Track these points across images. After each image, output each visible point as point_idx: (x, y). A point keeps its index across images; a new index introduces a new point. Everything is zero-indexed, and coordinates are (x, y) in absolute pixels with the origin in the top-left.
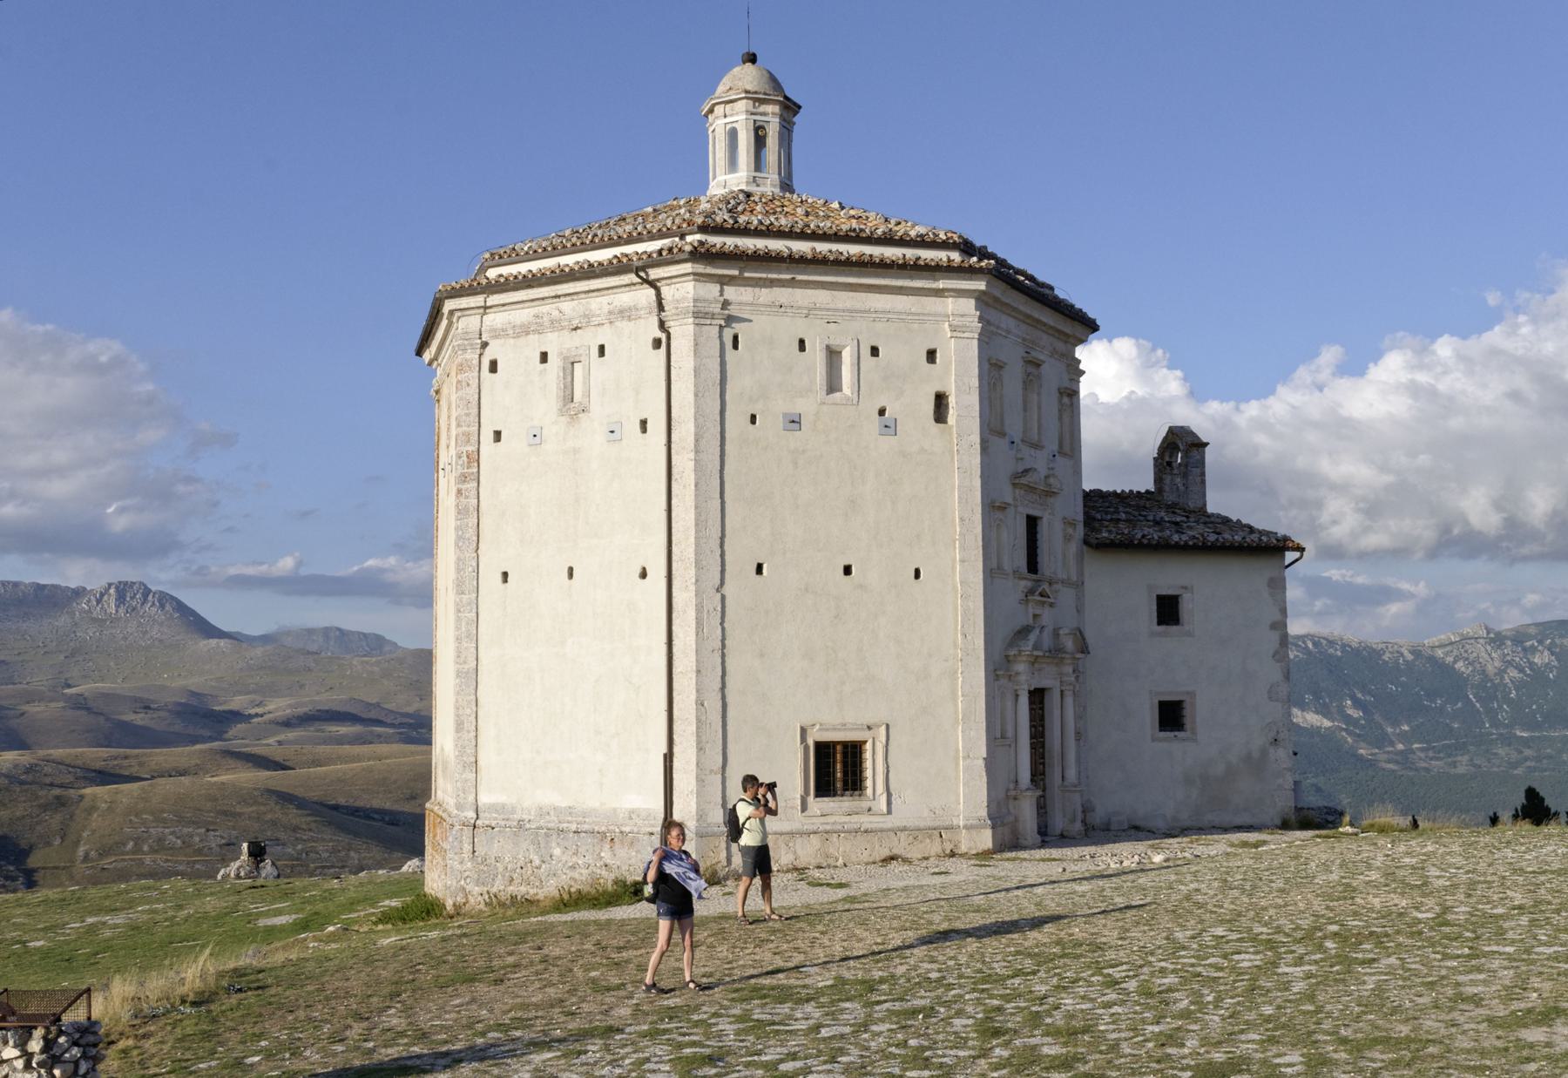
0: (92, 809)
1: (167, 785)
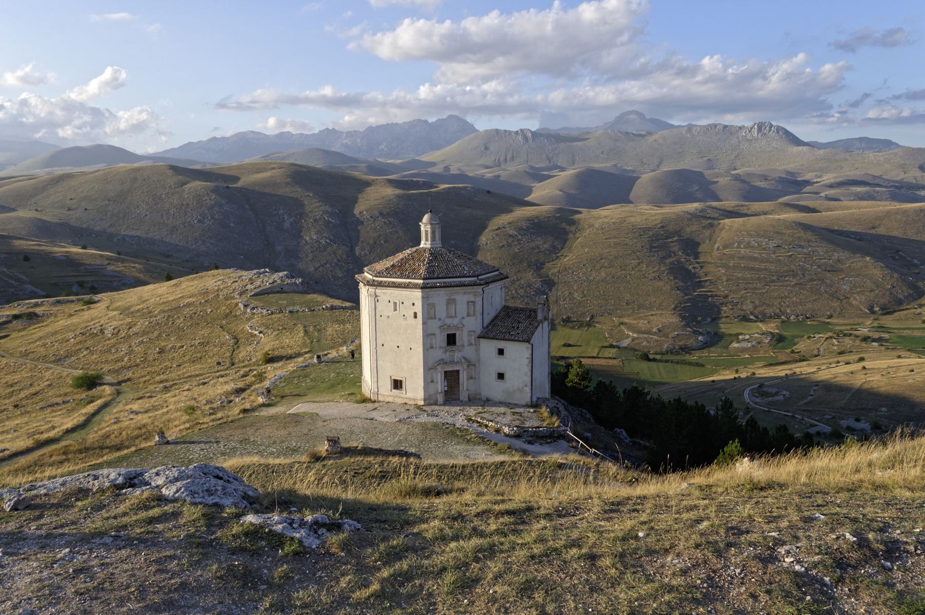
0: (723, 228)
1: (753, 219)
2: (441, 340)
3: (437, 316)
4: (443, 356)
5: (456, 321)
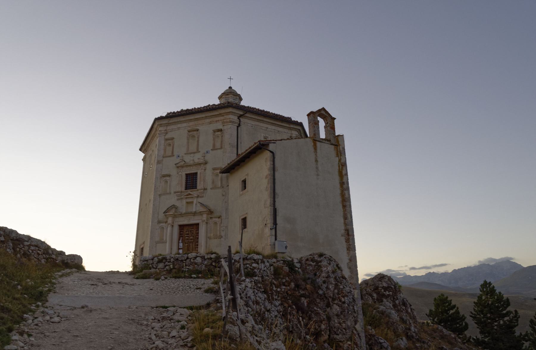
2: (177, 182)
3: (175, 153)
4: (178, 204)
5: (197, 158)
